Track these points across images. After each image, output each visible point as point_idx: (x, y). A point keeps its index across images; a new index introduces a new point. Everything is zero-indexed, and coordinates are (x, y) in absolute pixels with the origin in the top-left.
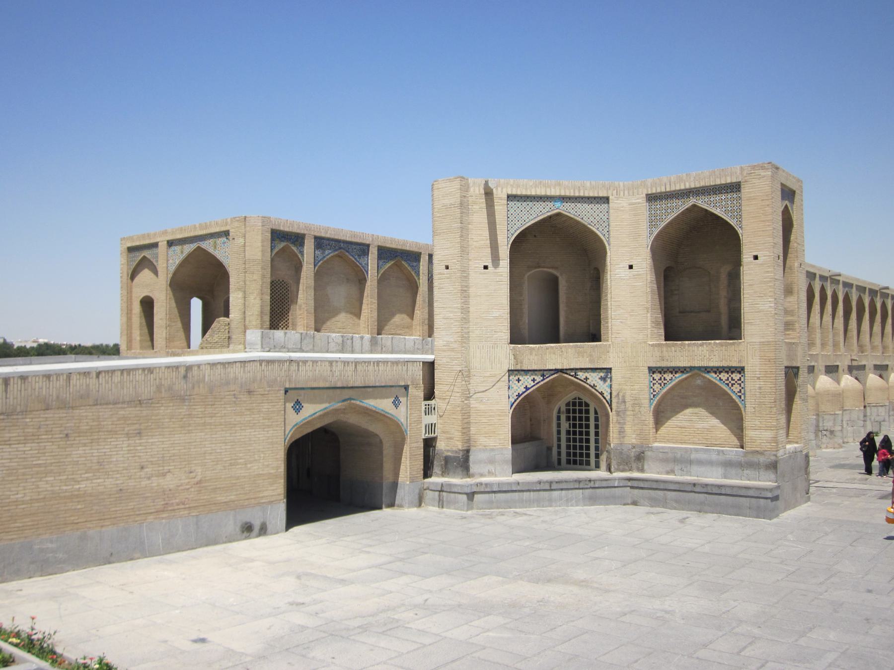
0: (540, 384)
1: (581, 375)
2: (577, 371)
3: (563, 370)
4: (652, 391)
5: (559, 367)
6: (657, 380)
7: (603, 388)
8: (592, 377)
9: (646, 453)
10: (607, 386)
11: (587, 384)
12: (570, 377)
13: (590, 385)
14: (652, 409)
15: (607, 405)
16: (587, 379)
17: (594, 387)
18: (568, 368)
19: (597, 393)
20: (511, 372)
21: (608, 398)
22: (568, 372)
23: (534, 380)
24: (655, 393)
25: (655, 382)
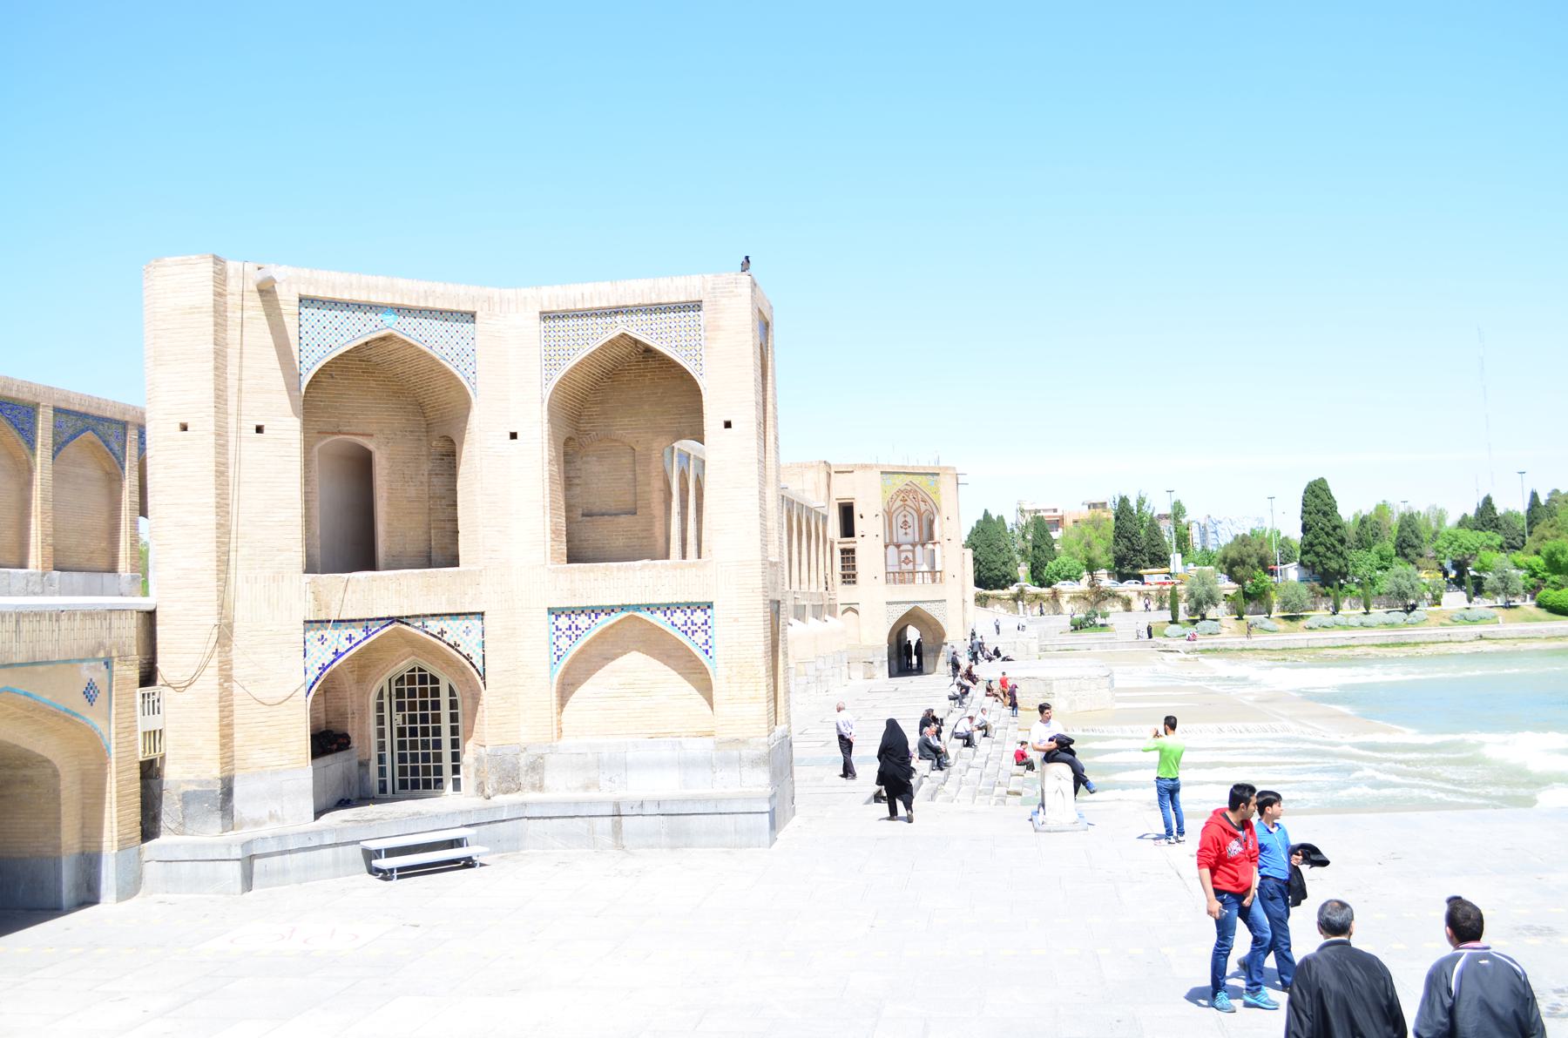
1: (434, 626)
3: (402, 617)
4: (555, 648)
6: (564, 630)
9: (546, 757)
11: (444, 641)
12: (413, 630)
13: (448, 644)
15: (478, 678)
16: (442, 632)
17: (454, 646)
21: (479, 665)
22: (409, 621)
24: (559, 653)
25: (559, 633)
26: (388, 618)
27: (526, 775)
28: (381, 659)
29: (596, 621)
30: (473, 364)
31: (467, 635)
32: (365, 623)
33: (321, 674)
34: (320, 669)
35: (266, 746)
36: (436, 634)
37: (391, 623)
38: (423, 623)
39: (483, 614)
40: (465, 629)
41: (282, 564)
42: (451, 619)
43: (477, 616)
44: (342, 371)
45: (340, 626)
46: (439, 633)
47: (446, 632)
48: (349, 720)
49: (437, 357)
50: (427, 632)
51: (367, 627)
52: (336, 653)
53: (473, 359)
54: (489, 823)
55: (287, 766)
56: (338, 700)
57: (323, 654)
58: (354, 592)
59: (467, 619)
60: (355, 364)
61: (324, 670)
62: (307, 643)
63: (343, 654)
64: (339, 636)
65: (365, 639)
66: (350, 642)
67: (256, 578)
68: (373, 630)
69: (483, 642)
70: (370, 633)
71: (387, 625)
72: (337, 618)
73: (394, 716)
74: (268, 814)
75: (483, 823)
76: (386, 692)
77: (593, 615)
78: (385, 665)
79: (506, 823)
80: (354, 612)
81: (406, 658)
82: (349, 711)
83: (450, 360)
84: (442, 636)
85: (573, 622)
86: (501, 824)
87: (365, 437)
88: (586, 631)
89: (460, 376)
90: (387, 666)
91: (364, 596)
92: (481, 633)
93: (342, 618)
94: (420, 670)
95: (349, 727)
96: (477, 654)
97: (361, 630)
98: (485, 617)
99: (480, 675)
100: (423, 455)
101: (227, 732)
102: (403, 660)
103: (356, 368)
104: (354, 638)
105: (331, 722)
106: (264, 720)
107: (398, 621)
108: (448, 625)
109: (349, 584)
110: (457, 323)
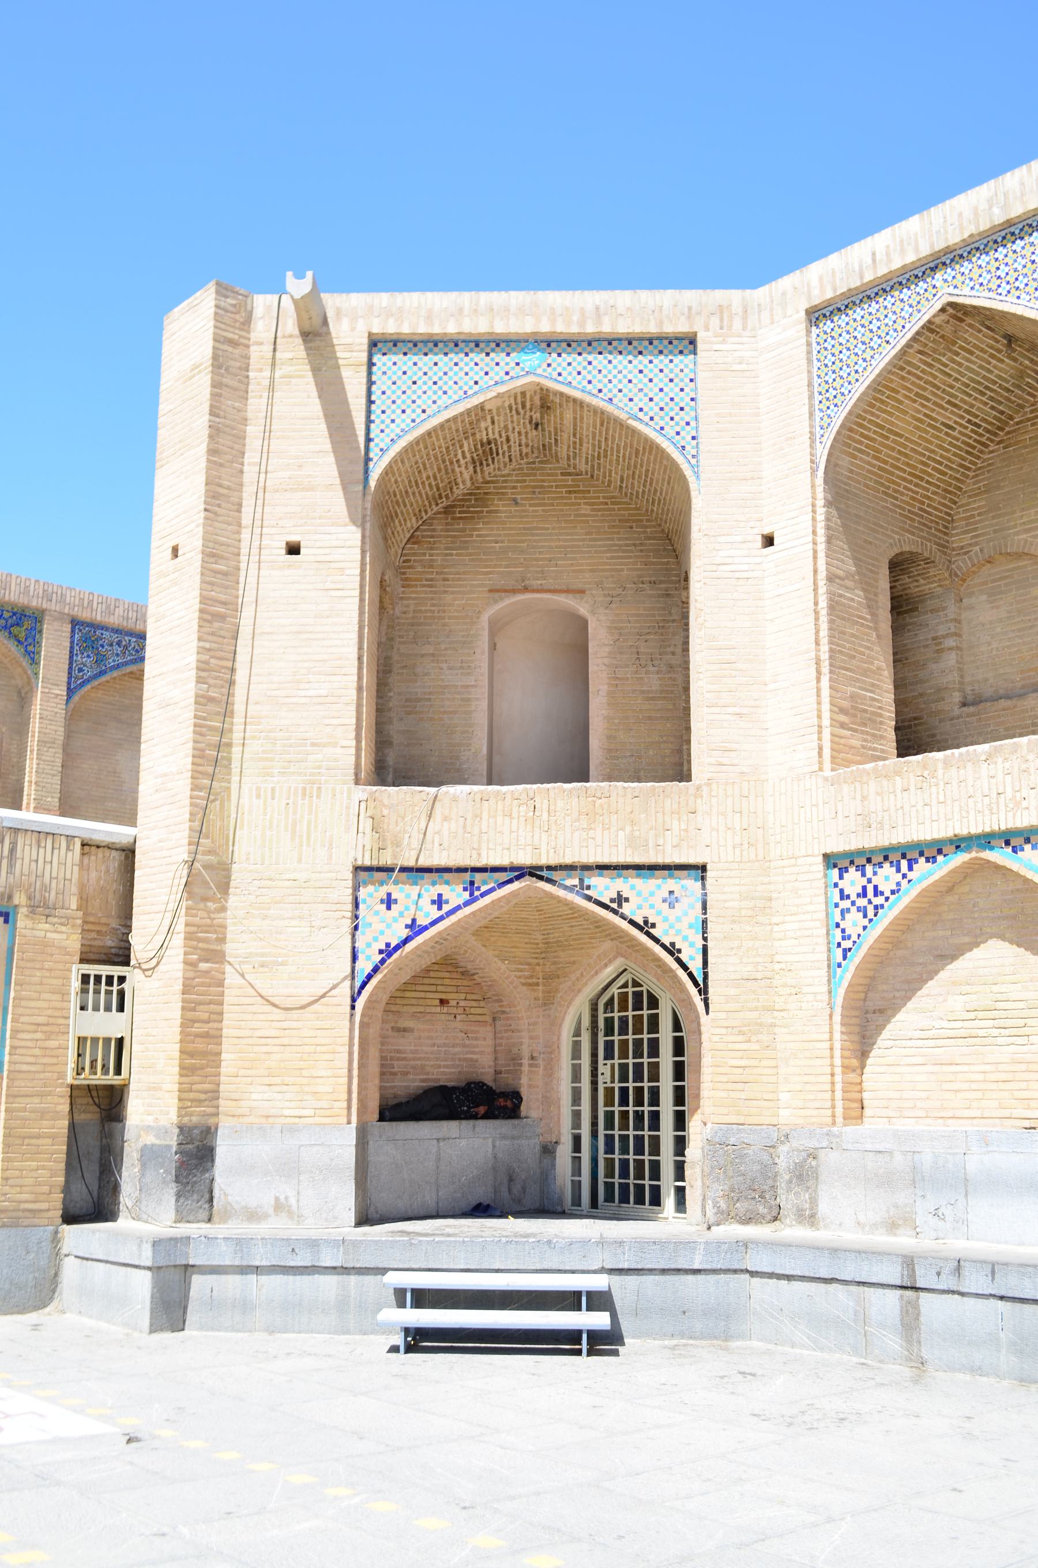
0: (460, 915)
1: (604, 887)
2: (586, 873)
3: (540, 868)
4: (838, 935)
5: (525, 859)
6: (853, 897)
7: (678, 932)
8: (639, 894)
9: (822, 1154)
10: (690, 927)
11: (623, 917)
12: (561, 893)
13: (632, 922)
14: (839, 1000)
15: (693, 991)
16: (620, 899)
17: (645, 927)
18: (553, 862)
19: (657, 949)
20: (363, 875)
21: (696, 967)
23: (439, 902)
24: (847, 944)
25: (845, 904)
26: (513, 869)
27: (789, 1190)
28: (574, 963)
29: (910, 875)
30: (693, 423)
31: (671, 906)
32: (467, 876)
33: (383, 961)
34: (381, 952)
35: (278, 1080)
36: (607, 902)
37: (518, 878)
38: (581, 881)
39: (703, 868)
40: (667, 895)
41: (320, 767)
42: (638, 876)
43: (693, 872)
44: (534, 493)
45: (422, 878)
46: (612, 901)
47: (627, 900)
48: (525, 1068)
49: (623, 416)
50: (589, 898)
51: (472, 883)
52: (412, 925)
53: (693, 414)
54: (664, 1271)
55: (310, 1120)
56: (510, 1033)
57: (389, 926)
58: (446, 819)
59: (671, 877)
60: (555, 481)
61: (389, 955)
62: (361, 906)
63: (425, 928)
64: (419, 895)
65: (467, 904)
66: (440, 908)
67: (273, 789)
68: (484, 889)
69: (705, 922)
70: (477, 893)
71: (510, 881)
72: (411, 863)
73: (601, 1069)
74: (273, 1202)
75: (651, 1271)
76: (586, 1022)
77: (904, 864)
78: (579, 972)
79: (700, 1277)
80: (445, 853)
81: (610, 961)
82: (526, 1054)
83: (647, 419)
84: (620, 905)
85: (869, 881)
86: (690, 1278)
87: (570, 596)
88: (892, 897)
89: (665, 444)
90: (582, 975)
91: (465, 827)
92: (699, 905)
93: (423, 862)
94: (636, 984)
95: (524, 1081)
96: (692, 945)
97: (461, 886)
98: (709, 874)
99: (696, 983)
100: (674, 621)
101: (200, 1045)
102: (606, 966)
103: (557, 487)
104: (447, 902)
105: (501, 1073)
106: (273, 1033)
107: (532, 875)
108: (633, 888)
109: (437, 804)
110: (662, 357)
